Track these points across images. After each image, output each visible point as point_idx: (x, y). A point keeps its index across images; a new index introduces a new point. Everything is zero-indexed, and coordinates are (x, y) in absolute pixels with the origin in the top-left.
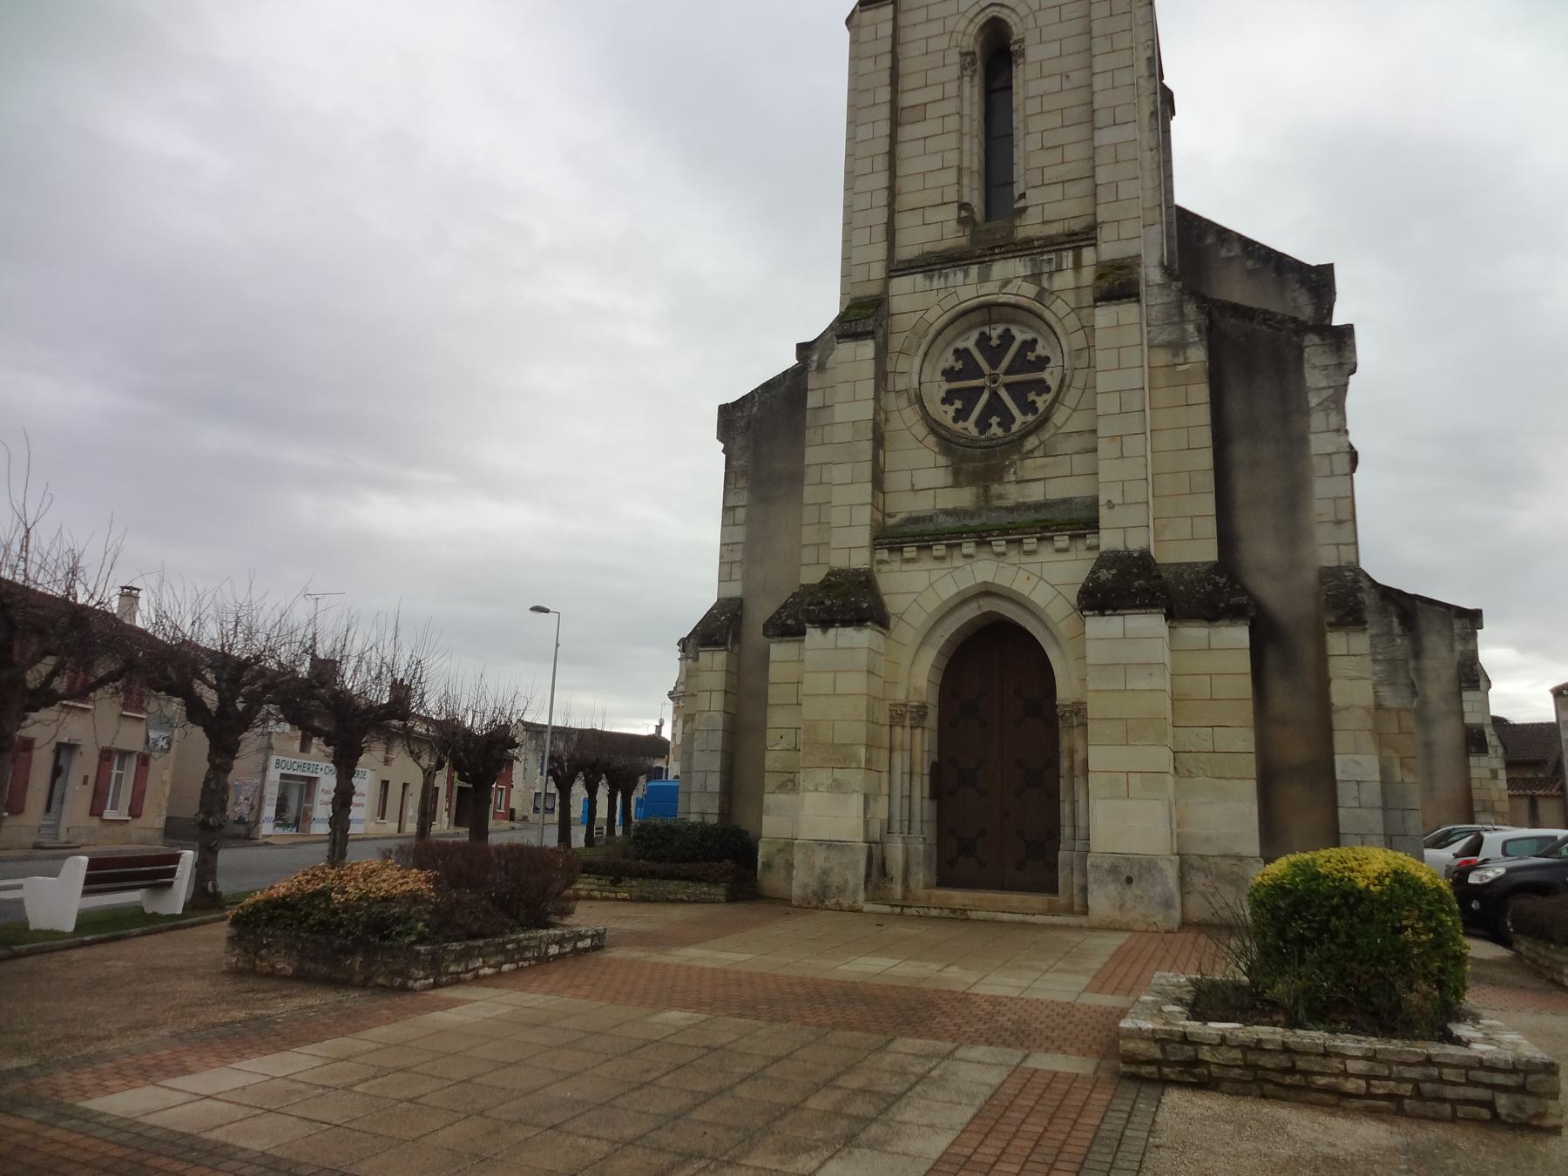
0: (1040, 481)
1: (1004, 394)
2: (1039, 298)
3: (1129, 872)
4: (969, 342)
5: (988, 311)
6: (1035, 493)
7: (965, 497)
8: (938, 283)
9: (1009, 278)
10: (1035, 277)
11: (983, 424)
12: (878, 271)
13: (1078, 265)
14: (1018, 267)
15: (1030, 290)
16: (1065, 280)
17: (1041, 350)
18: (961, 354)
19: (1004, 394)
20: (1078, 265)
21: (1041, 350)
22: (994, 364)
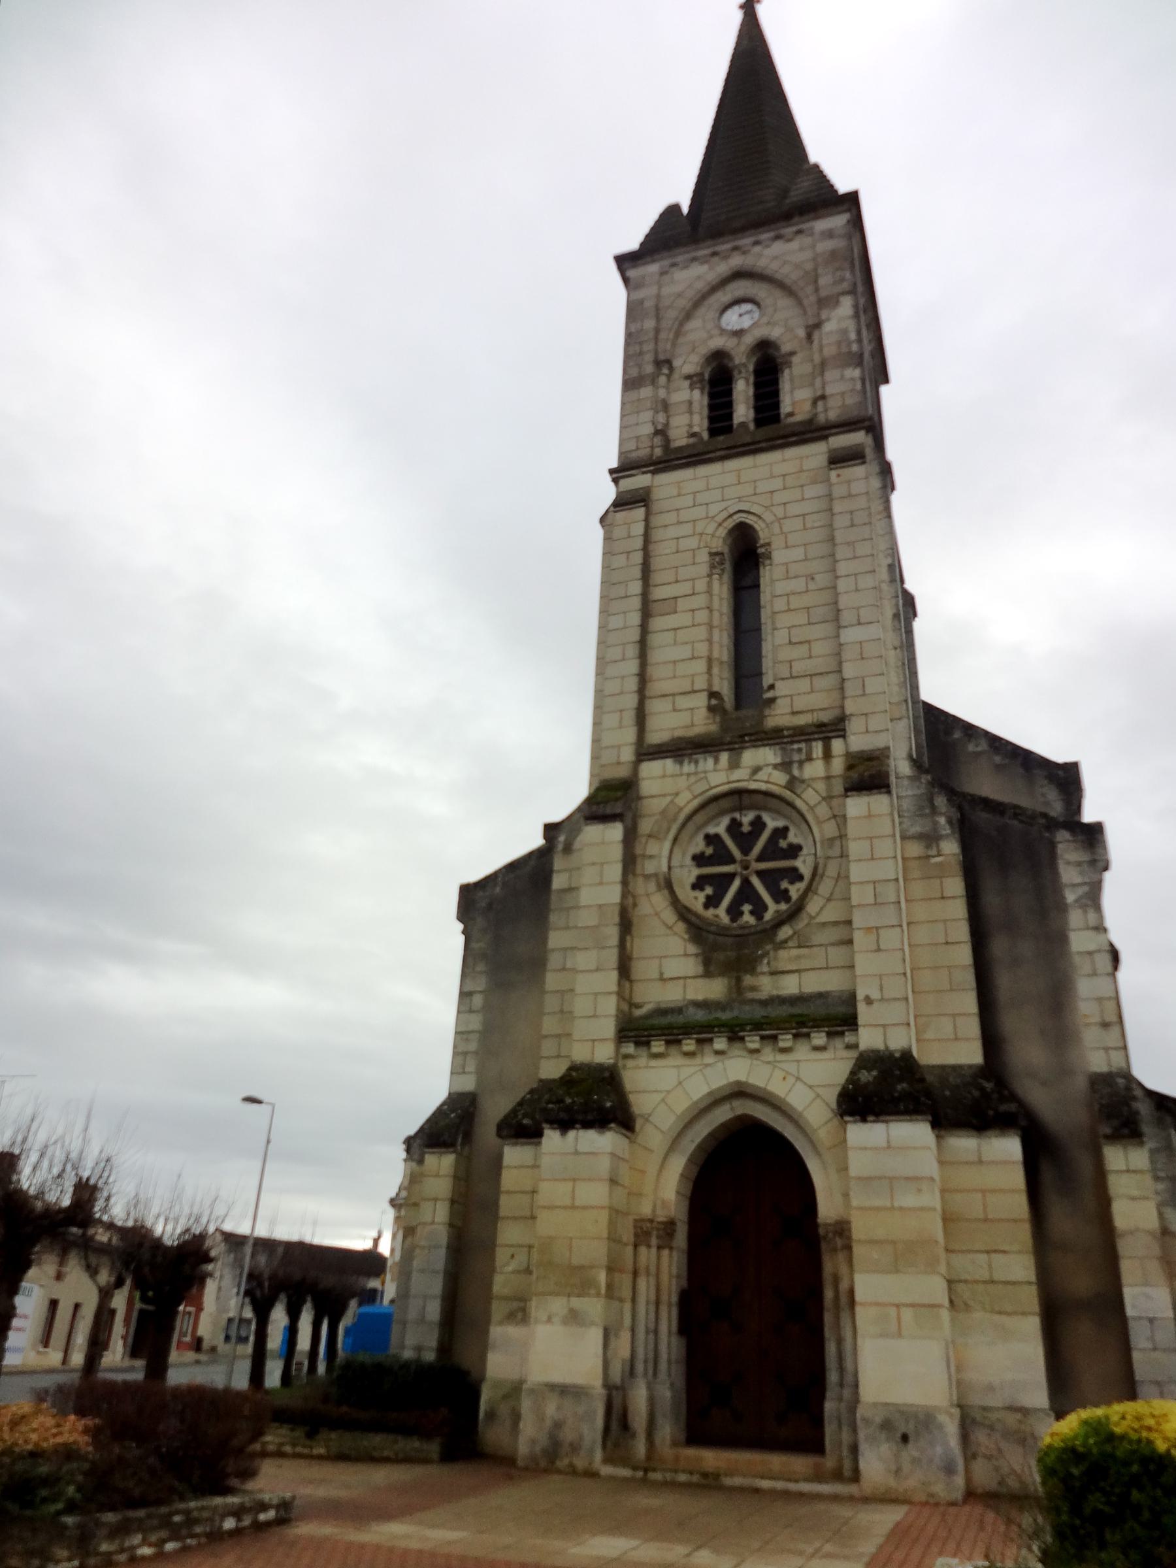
0: (795, 974)
1: (756, 881)
2: (792, 784)
3: (905, 1429)
4: (720, 828)
5: (739, 797)
6: (790, 986)
7: (715, 989)
8: (688, 768)
9: (759, 766)
10: (785, 766)
11: (734, 912)
12: (628, 755)
13: (827, 755)
14: (767, 755)
15: (780, 778)
16: (815, 769)
17: (793, 837)
18: (711, 839)
19: (756, 881)
20: (827, 755)
21: (793, 837)
22: (746, 851)
